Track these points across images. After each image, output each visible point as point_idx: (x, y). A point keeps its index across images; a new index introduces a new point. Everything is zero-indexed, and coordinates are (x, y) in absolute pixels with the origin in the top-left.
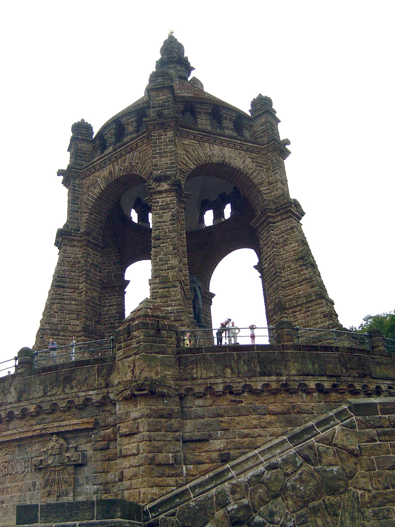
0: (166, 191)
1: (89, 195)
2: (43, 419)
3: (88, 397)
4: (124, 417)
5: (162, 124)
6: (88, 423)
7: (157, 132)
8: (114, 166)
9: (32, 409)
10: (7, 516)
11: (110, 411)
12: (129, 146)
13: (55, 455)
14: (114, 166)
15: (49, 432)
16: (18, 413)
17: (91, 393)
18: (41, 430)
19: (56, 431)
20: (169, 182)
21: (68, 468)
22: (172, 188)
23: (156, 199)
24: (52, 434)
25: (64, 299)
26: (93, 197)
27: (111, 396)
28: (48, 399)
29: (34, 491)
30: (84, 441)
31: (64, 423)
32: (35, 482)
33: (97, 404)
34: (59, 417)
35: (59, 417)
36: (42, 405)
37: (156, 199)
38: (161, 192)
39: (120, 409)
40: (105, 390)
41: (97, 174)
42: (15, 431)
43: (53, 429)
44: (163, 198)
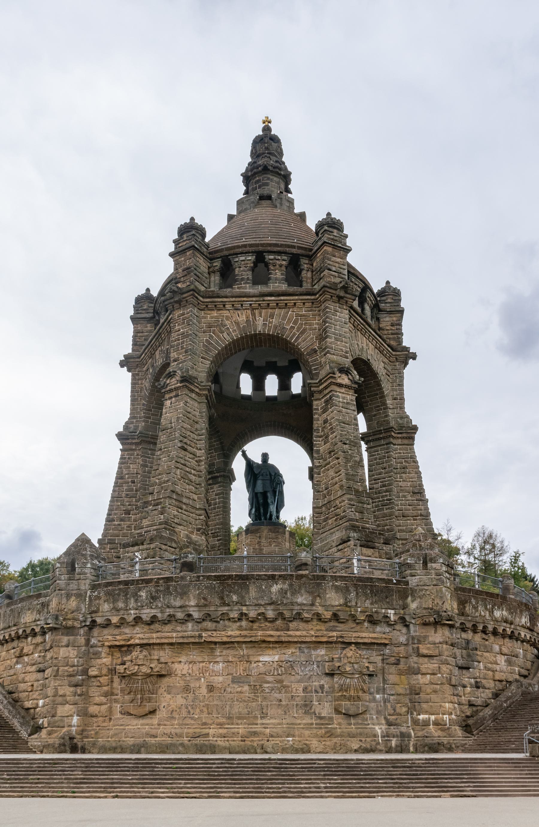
0: (346, 386)
1: (211, 337)
2: (334, 626)
3: (386, 615)
4: (422, 640)
5: (340, 298)
6: (386, 639)
7: (333, 304)
8: (254, 315)
9: (328, 615)
10: (288, 714)
11: (400, 631)
12: (284, 300)
13: (353, 663)
14: (254, 315)
15: (347, 641)
16: (309, 616)
17: (389, 611)
18: (337, 637)
19: (353, 641)
20: (350, 377)
21: (363, 676)
22: (353, 385)
23: (336, 392)
24: (350, 644)
25: (185, 465)
26: (217, 343)
27: (407, 618)
28: (348, 609)
29: (322, 693)
30: (375, 653)
31: (364, 635)
32: (323, 685)
33: (393, 623)
34: (352, 628)
35: (352, 628)
36: (339, 613)
37: (336, 392)
38: (340, 385)
39: (415, 631)
40: (402, 612)
41: (226, 313)
42: (304, 633)
43: (350, 638)
44: (343, 393)
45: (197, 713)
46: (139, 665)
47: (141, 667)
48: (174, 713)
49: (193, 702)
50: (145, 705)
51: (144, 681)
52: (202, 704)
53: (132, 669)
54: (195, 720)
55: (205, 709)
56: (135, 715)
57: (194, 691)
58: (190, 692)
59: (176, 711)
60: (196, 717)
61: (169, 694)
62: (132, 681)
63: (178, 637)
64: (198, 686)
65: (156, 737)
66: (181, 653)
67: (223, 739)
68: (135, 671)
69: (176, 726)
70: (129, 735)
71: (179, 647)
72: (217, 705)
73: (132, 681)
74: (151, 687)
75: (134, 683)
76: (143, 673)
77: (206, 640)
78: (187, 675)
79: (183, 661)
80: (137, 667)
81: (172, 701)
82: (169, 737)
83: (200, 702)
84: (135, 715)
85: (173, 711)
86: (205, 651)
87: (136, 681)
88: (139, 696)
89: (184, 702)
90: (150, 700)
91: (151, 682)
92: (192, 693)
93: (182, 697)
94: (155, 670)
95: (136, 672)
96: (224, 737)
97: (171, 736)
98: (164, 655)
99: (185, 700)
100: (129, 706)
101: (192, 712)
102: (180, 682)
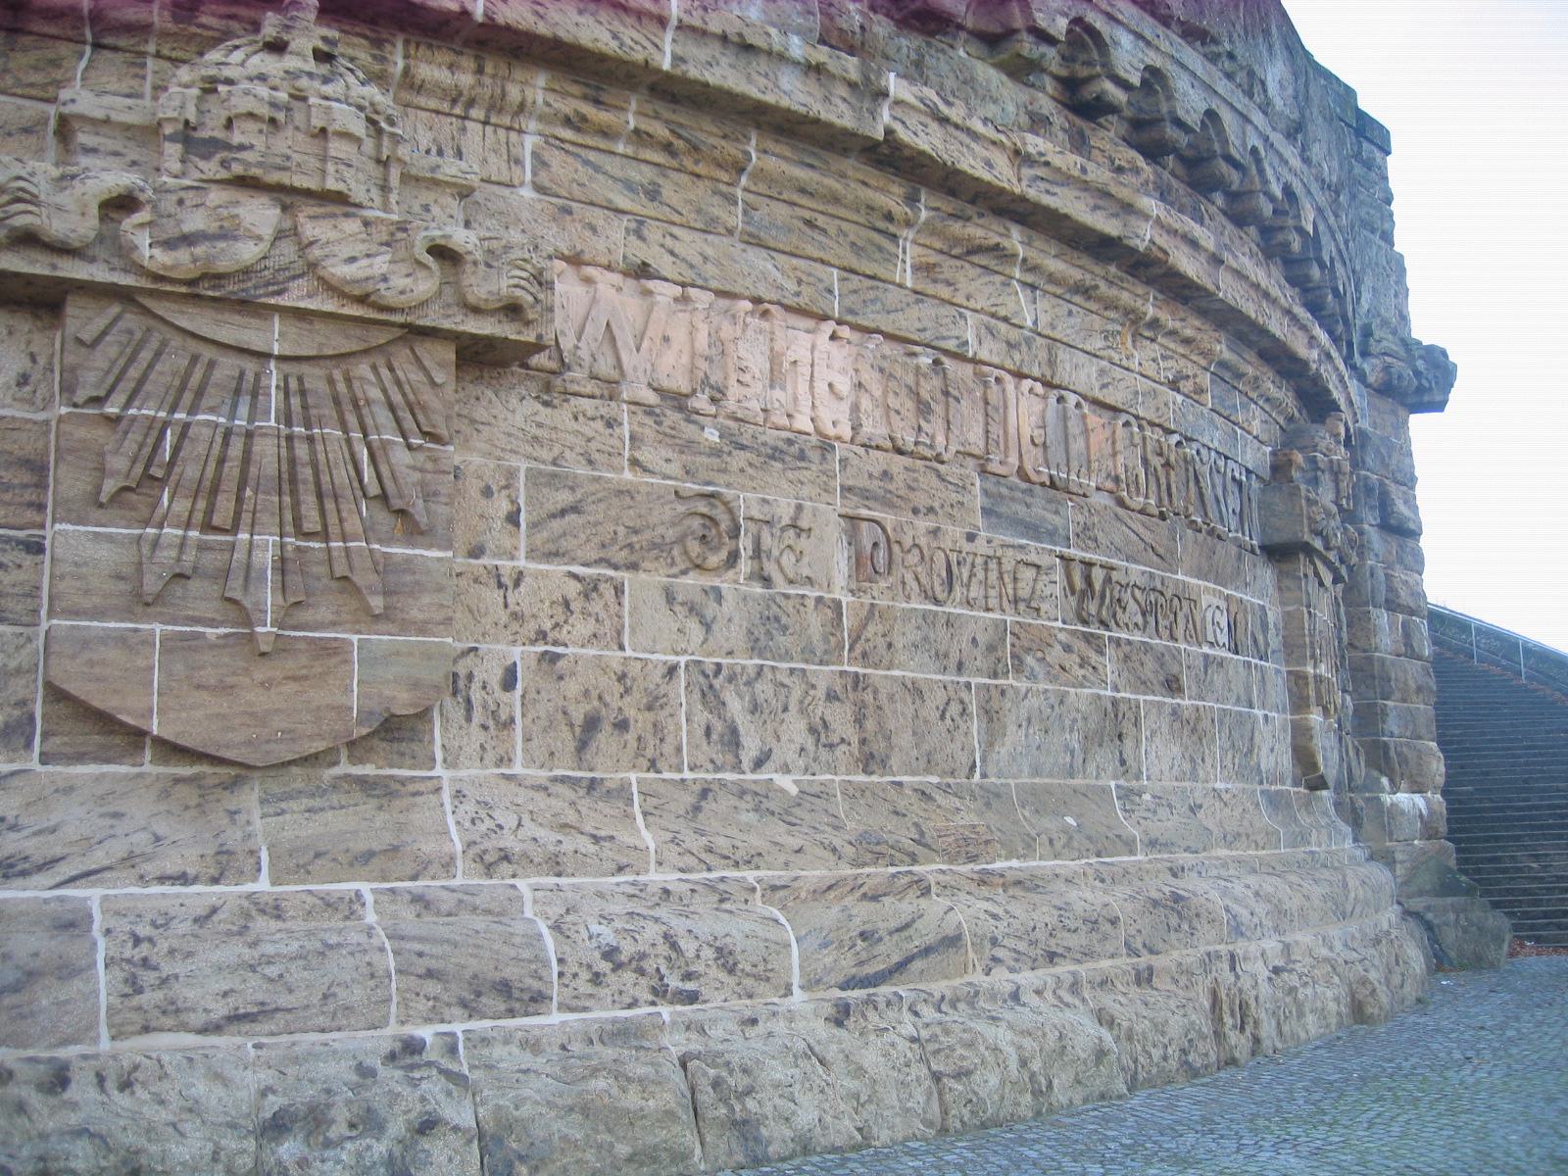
45: (785, 752)
46: (287, 196)
47: (314, 228)
48: (605, 738)
49: (755, 648)
50: (333, 651)
51: (315, 378)
52: (824, 675)
53: (195, 222)
54: (787, 813)
55: (841, 719)
56: (171, 750)
57: (757, 553)
58: (733, 558)
59: (622, 726)
60: (787, 783)
61: (552, 555)
62: (174, 362)
63: (701, 34)
64: (784, 511)
65: (537, 1000)
66: (653, 194)
67: (1044, 975)
68: (247, 252)
69: (655, 877)
70: (188, 994)
71: (661, 131)
72: (916, 691)
73: (174, 362)
74: (401, 457)
75: (188, 392)
76: (332, 288)
77: (903, 135)
78: (701, 402)
79: (663, 263)
80: (260, 214)
81: (582, 628)
82: (660, 992)
83: (808, 654)
84: (171, 750)
85: (592, 724)
86: (831, 226)
87: (228, 366)
88: (266, 546)
89: (689, 646)
90: (381, 599)
91: (410, 415)
92: (745, 566)
93: (670, 597)
94: (482, 286)
95: (246, 272)
96: (1052, 957)
97: (674, 982)
98: (497, 167)
99: (695, 630)
100: (121, 640)
101: (751, 747)
102: (645, 455)
